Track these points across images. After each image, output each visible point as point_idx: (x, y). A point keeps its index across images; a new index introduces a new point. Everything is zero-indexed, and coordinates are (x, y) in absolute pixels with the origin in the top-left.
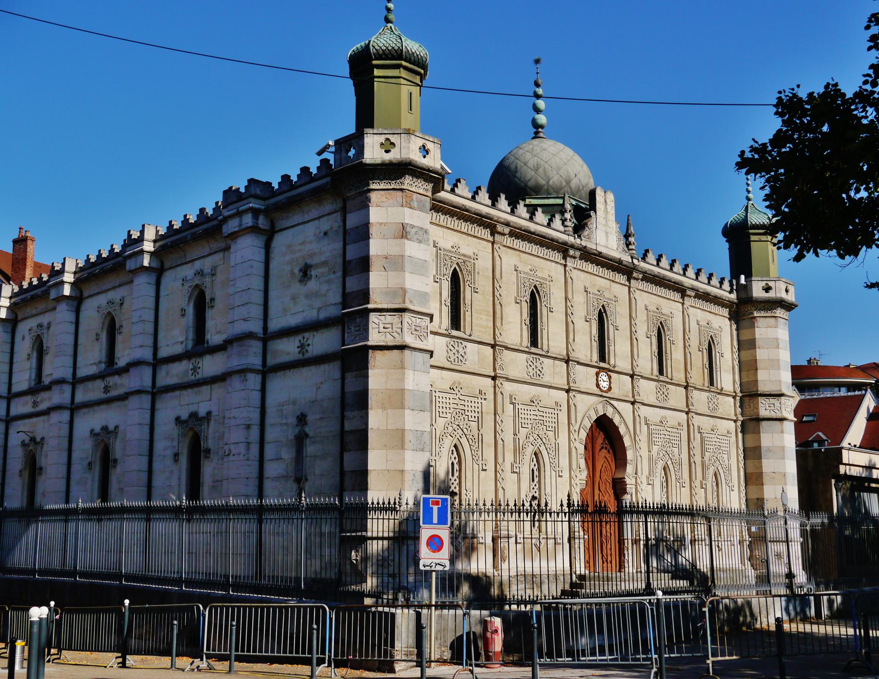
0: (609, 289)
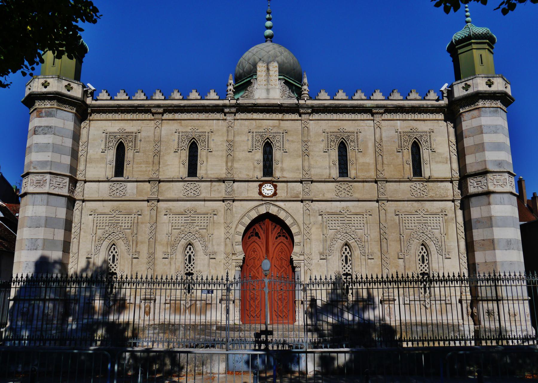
0: (279, 127)
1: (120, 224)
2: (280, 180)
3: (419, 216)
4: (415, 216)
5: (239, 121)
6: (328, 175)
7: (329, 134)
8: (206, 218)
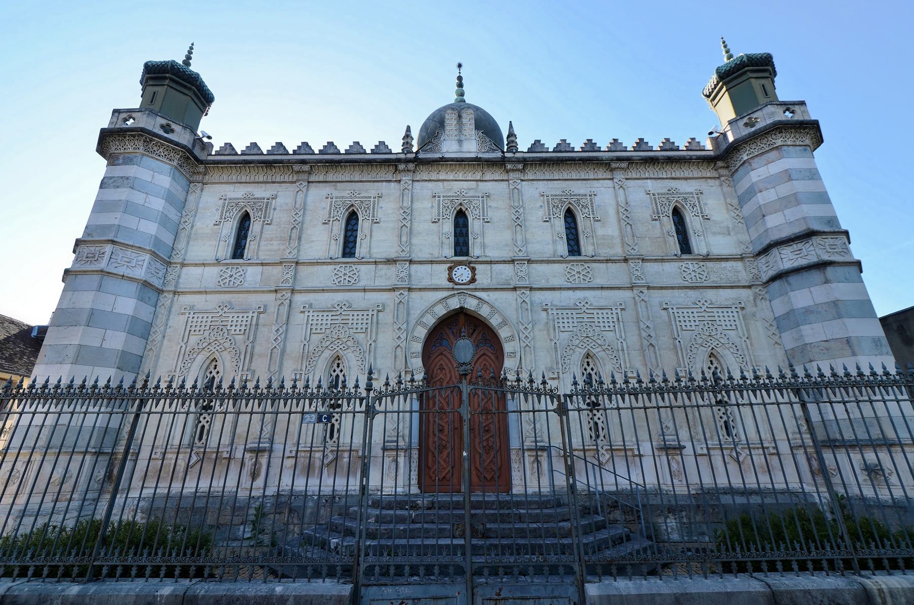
0: (476, 189)
1: (229, 328)
2: (480, 259)
3: (699, 310)
4: (695, 311)
5: (420, 183)
6: (552, 252)
7: (550, 198)
8: (365, 317)
